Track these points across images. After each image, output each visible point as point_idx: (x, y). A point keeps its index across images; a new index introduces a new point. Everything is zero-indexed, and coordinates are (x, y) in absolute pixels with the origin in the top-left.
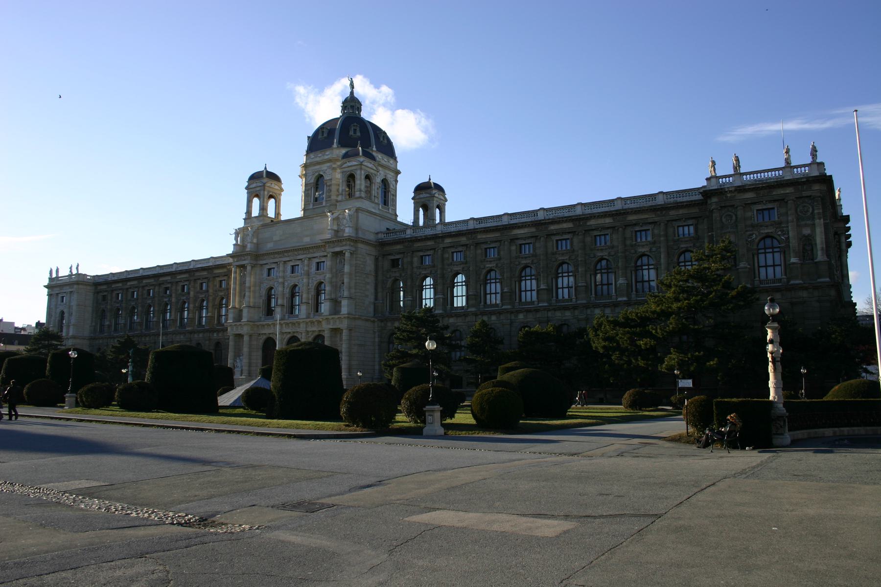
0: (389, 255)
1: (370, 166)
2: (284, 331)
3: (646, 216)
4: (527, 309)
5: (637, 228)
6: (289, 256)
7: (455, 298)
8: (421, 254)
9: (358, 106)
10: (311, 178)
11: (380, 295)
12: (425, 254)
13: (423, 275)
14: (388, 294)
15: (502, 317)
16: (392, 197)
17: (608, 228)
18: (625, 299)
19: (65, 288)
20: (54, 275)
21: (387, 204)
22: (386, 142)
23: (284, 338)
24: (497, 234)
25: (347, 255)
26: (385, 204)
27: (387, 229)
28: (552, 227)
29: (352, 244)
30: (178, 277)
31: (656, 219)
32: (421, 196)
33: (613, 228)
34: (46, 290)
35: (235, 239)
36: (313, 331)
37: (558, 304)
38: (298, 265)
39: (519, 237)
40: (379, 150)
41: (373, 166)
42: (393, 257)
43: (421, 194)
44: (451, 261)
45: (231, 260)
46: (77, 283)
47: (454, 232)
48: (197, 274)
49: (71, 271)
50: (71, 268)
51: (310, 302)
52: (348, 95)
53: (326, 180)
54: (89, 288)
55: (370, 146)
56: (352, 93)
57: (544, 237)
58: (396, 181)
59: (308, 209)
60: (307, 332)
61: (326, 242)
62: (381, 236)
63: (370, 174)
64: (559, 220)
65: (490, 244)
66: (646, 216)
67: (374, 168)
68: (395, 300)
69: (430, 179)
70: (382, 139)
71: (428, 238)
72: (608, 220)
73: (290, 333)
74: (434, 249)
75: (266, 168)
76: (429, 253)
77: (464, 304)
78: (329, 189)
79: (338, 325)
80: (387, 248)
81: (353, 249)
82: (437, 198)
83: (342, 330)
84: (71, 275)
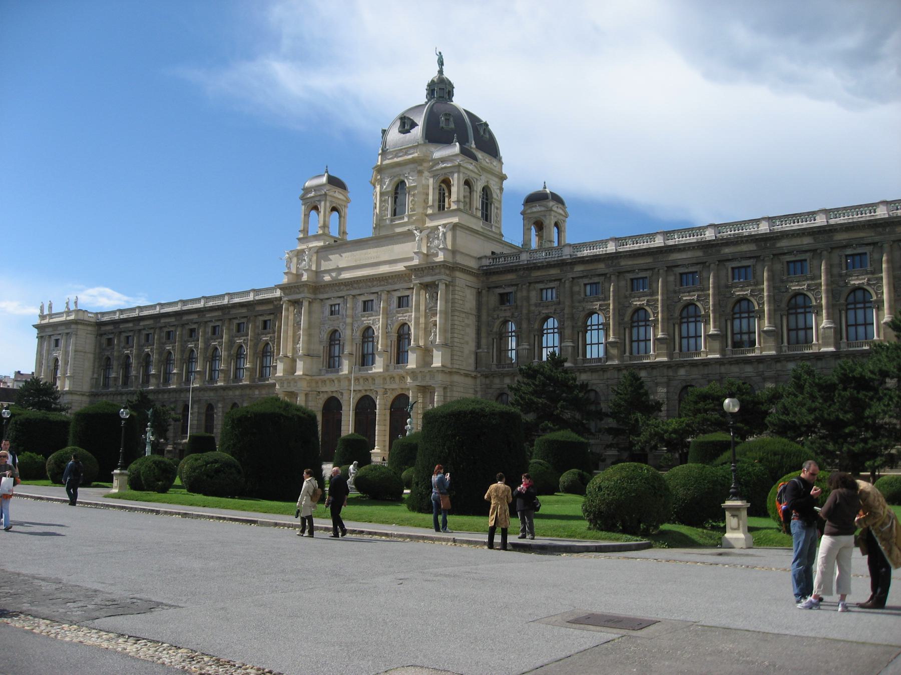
0: (496, 287)
1: (471, 167)
3: (862, 235)
4: (690, 362)
5: (849, 251)
6: (360, 288)
7: (588, 347)
8: (541, 286)
9: (450, 89)
10: (388, 185)
11: (484, 341)
12: (547, 286)
13: (544, 315)
14: (495, 340)
15: (655, 373)
16: (495, 210)
17: (806, 251)
18: (832, 349)
19: (59, 328)
20: (46, 312)
21: (489, 219)
22: (488, 136)
24: (649, 260)
25: (442, 287)
26: (486, 220)
27: (493, 253)
28: (727, 250)
29: (448, 272)
30: (207, 316)
31: (877, 239)
32: (534, 210)
33: (814, 251)
34: (36, 331)
35: (287, 266)
37: (734, 356)
38: (372, 301)
39: (679, 263)
40: (479, 147)
41: (474, 168)
42: (501, 291)
43: (533, 207)
44: (583, 296)
46: (76, 322)
47: (587, 257)
48: (234, 311)
49: (67, 307)
50: (67, 303)
51: (389, 350)
53: (409, 187)
54: (90, 328)
55: (468, 142)
56: (441, 72)
57: (714, 263)
58: (501, 189)
60: (385, 393)
61: (411, 270)
62: (486, 262)
64: (736, 240)
65: (638, 274)
66: (862, 235)
67: (476, 170)
68: (502, 350)
69: (545, 188)
71: (551, 265)
72: (807, 241)
73: (360, 391)
74: (560, 280)
76: (552, 285)
77: (602, 354)
78: (413, 200)
79: (428, 382)
80: (494, 278)
81: (449, 279)
82: (556, 212)
83: (434, 388)
84: (68, 313)
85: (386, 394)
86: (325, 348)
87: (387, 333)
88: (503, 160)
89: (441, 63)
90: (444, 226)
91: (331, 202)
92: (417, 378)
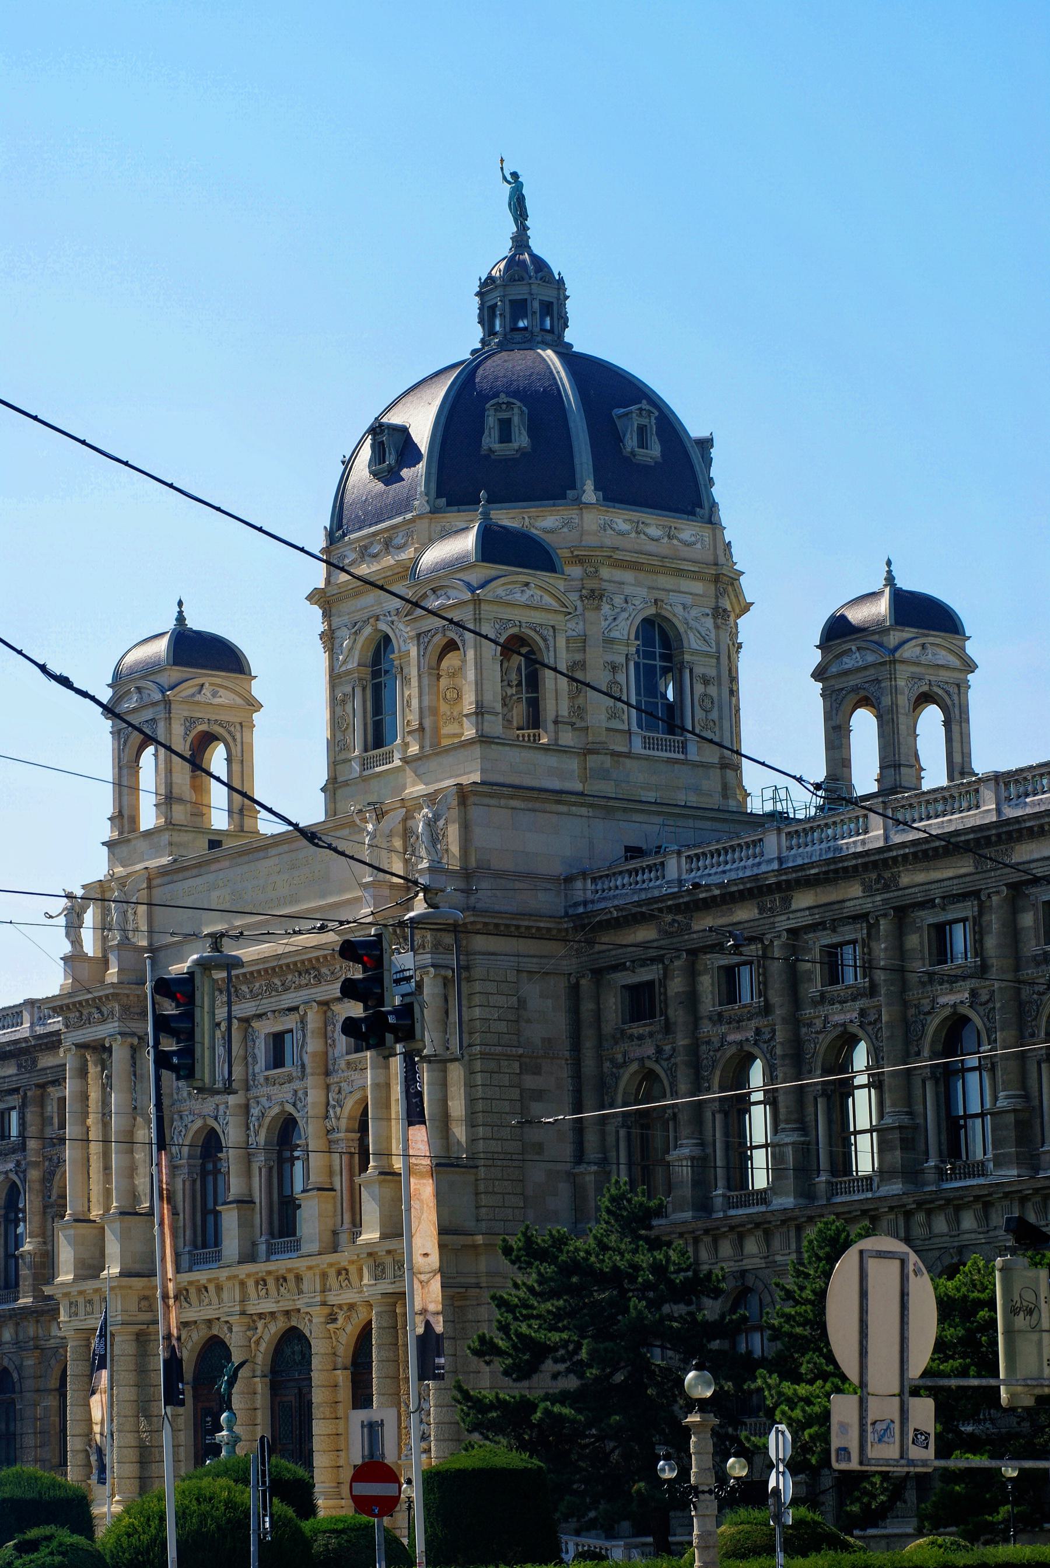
2: (251, 1310)
6: (254, 996)
9: (548, 294)
16: (699, 688)
22: (655, 450)
23: (257, 1343)
27: (633, 852)
32: (849, 663)
36: (352, 1307)
45: (56, 1023)
52: (504, 248)
55: (573, 487)
56: (521, 241)
59: (346, 784)
62: (582, 890)
63: (532, 634)
70: (631, 442)
75: (181, 618)
85: (335, 1320)
86: (187, 1184)
87: (328, 1131)
88: (726, 516)
89: (518, 207)
90: (431, 799)
91: (191, 722)
92: (383, 1271)
